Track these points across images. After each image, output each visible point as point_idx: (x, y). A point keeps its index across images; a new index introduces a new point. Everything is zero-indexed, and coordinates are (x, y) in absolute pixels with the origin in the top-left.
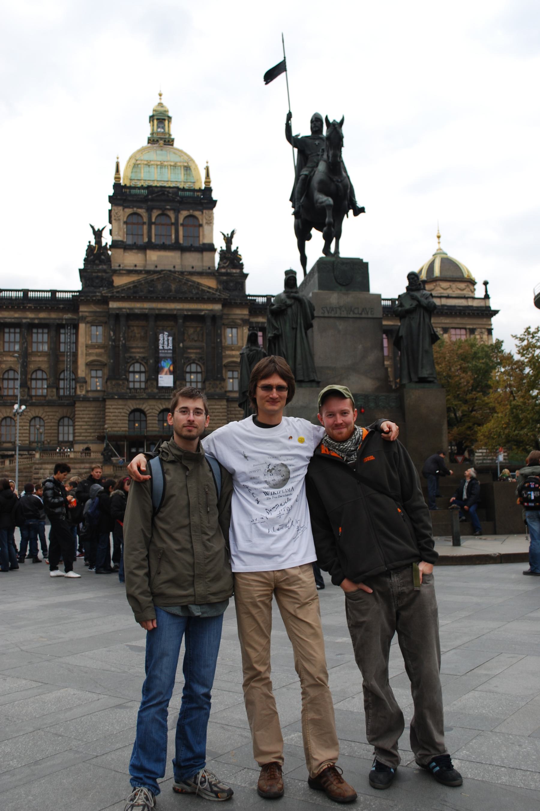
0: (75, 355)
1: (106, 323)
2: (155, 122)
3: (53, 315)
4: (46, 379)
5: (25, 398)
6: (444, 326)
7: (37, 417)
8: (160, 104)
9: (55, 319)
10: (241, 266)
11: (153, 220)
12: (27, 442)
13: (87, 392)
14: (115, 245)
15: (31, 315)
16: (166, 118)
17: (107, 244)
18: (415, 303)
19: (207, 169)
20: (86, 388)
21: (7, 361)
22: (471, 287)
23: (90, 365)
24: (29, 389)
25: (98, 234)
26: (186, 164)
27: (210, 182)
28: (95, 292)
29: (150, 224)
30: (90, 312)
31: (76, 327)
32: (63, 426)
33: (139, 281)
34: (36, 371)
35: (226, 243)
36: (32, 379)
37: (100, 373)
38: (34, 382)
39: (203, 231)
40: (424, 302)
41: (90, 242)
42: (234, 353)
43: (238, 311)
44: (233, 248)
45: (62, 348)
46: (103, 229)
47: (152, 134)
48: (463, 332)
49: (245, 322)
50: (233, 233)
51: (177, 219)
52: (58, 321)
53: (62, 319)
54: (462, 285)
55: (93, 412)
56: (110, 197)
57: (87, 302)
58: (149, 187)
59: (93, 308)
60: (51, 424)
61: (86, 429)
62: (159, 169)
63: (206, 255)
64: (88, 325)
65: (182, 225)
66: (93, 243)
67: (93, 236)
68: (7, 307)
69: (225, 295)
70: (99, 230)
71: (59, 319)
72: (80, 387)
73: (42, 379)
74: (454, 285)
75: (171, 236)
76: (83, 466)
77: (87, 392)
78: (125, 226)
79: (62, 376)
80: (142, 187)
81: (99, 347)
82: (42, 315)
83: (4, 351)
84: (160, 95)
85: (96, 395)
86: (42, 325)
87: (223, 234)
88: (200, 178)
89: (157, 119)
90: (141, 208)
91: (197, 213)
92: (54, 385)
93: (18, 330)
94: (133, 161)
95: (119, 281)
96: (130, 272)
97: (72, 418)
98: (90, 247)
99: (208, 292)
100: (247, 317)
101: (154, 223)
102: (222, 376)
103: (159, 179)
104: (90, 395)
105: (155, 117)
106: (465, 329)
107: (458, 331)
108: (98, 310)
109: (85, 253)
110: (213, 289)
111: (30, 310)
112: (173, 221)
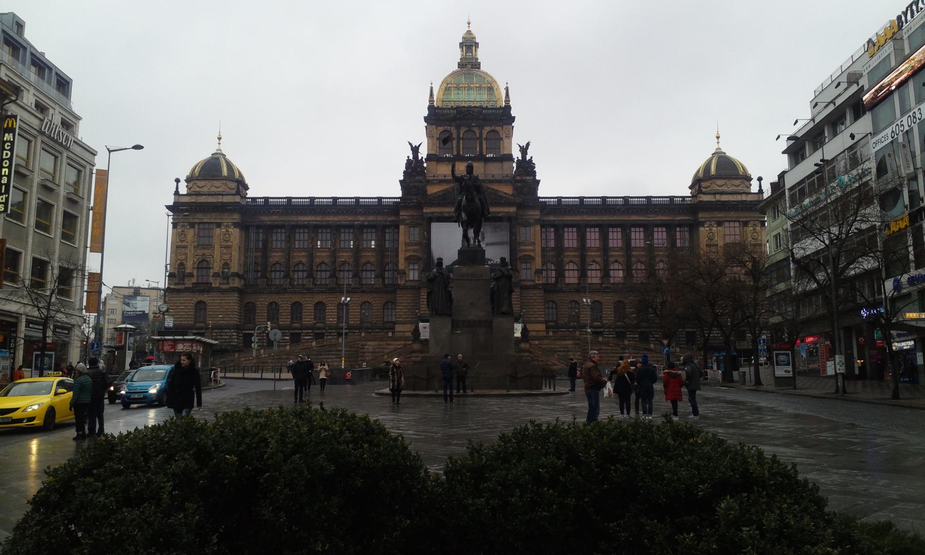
0: (397, 250)
1: (421, 224)
2: (464, 48)
3: (380, 218)
4: (374, 271)
5: (357, 286)
6: (717, 219)
7: (367, 302)
8: (469, 32)
9: (380, 221)
10: (534, 174)
11: (461, 136)
12: (359, 322)
13: (406, 281)
14: (430, 158)
15: (361, 218)
16: (474, 44)
17: (422, 158)
18: (501, 274)
19: (507, 89)
20: (405, 278)
21: (343, 256)
22: (747, 183)
23: (408, 259)
24: (360, 278)
25: (415, 150)
26: (489, 85)
27: (509, 101)
28: (413, 199)
29: (459, 139)
30: (407, 216)
31: (398, 227)
32: (388, 309)
33: (447, 190)
34: (365, 264)
35: (522, 154)
36: (363, 271)
37: (416, 267)
38: (364, 273)
39: (503, 144)
40: (506, 273)
41: (408, 157)
42: (527, 248)
43: (531, 213)
44: (528, 158)
45: (387, 245)
46: (419, 145)
47: (461, 59)
48: (737, 224)
49: (537, 221)
50: (528, 144)
51: (481, 134)
52: (385, 223)
53: (387, 221)
54: (737, 182)
55: (410, 298)
56: (425, 117)
57: (406, 208)
58: (457, 108)
59: (410, 212)
60: (378, 308)
61: (405, 312)
62: (466, 92)
63: (506, 164)
64: (407, 226)
65: (486, 139)
66: (411, 158)
67: (411, 152)
68: (342, 212)
69: (518, 200)
70: (416, 146)
71: (385, 221)
72: (400, 277)
73: (371, 271)
74: (728, 183)
75: (476, 148)
76: (399, 343)
77: (406, 281)
78: (438, 142)
79: (387, 268)
80: (452, 108)
81: (416, 244)
82: (371, 218)
83: (340, 248)
84: (469, 23)
85: (413, 284)
86: (372, 226)
87: (520, 146)
88: (502, 97)
89: (466, 46)
90: (450, 126)
91: (498, 129)
92: (381, 276)
93: (351, 230)
94: (445, 85)
95: (432, 190)
96: (441, 182)
97: (394, 303)
98: (408, 160)
99: (504, 197)
100: (538, 217)
101: (462, 138)
102: (517, 268)
103: (466, 100)
104: (408, 284)
105: (464, 44)
106: (739, 221)
107: (732, 224)
108: (415, 214)
109: (404, 166)
110: (508, 194)
111: (361, 214)
112: (478, 136)
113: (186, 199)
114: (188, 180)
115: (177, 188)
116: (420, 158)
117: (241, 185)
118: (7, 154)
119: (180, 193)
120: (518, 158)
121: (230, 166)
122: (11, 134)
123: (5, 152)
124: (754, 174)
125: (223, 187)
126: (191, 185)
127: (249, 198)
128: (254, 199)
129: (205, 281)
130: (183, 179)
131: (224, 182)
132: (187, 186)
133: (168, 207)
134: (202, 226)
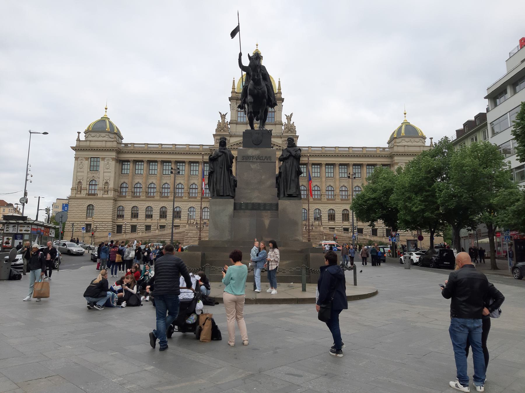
25: (223, 116)
44: (291, 123)
70: (224, 114)
114: (86, 132)
115: (79, 137)
116: (226, 122)
119: (80, 140)
120: (285, 123)
121: (111, 124)
124: (428, 135)
125: (107, 136)
126: (87, 135)
127: (123, 144)
128: (126, 145)
132: (85, 136)
133: (73, 148)
134: (92, 159)
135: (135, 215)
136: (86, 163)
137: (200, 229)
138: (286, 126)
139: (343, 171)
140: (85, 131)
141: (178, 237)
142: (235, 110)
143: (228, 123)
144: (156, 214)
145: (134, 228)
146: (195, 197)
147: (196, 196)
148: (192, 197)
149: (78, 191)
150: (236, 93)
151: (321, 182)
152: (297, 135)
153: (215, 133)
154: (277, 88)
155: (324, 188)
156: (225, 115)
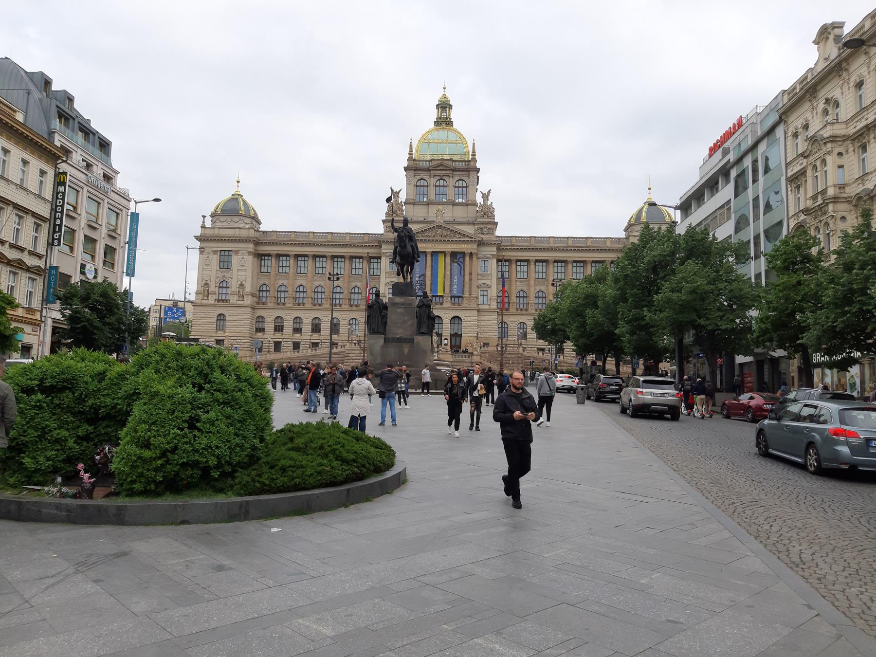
17: (401, 202)
27: (475, 155)
44: (489, 203)
113: (210, 232)
114: (212, 216)
115: (204, 222)
117: (255, 219)
118: (60, 202)
122: (63, 187)
123: (58, 200)
126: (214, 220)
127: (262, 231)
128: (264, 232)
129: (224, 298)
130: (208, 214)
131: (242, 218)
133: (197, 238)
135: (279, 329)
136: (215, 259)
137: (364, 349)
138: (481, 208)
139: (578, 271)
140: (212, 214)
141: (336, 359)
142: (412, 185)
143: (403, 203)
144: (307, 327)
145: (278, 346)
146: (358, 306)
147: (359, 303)
148: (354, 305)
149: (204, 296)
150: (414, 160)
151: (529, 285)
152: (496, 221)
153: (384, 218)
154: (471, 153)
155: (532, 295)
156: (398, 193)
